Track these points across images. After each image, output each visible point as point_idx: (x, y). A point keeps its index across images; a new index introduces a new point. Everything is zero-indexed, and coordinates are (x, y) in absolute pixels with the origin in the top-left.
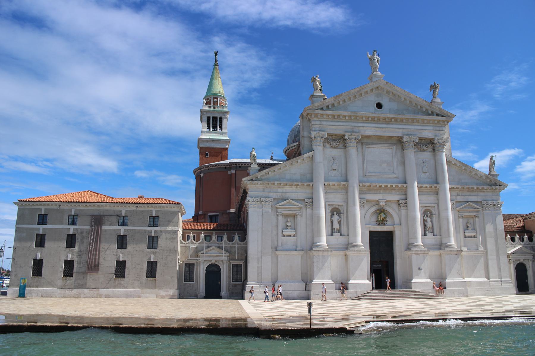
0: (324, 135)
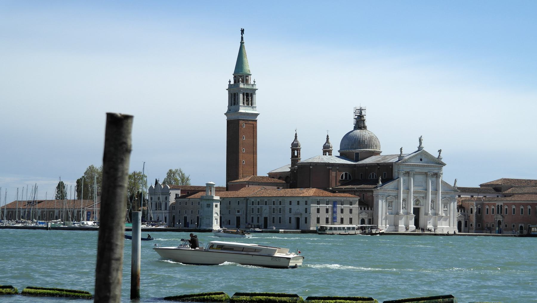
0: (404, 172)
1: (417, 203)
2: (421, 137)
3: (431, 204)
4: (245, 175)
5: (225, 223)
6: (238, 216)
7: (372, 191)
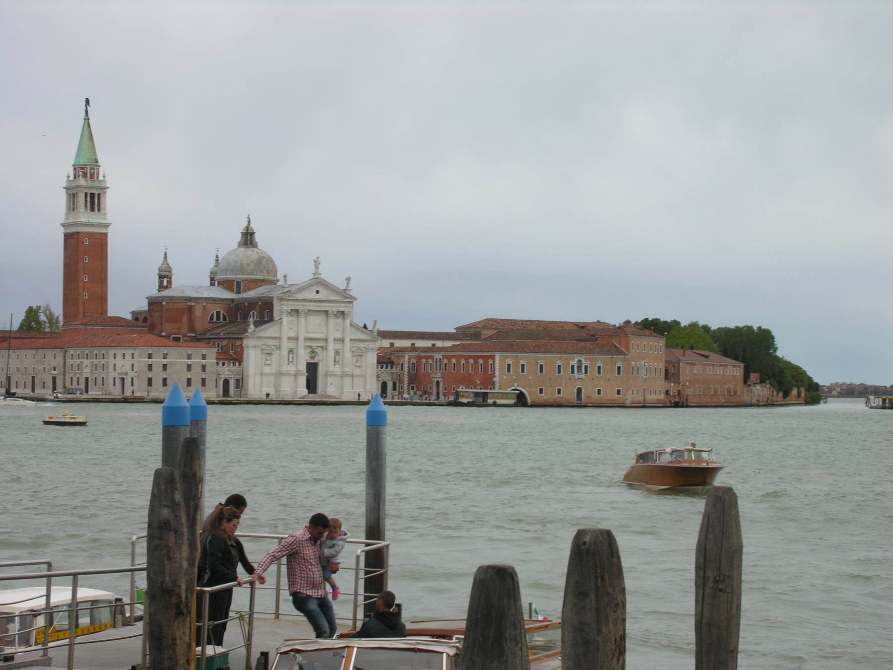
1: (312, 356)
2: (317, 259)
3: (335, 357)
4: (87, 315)
5: (39, 386)
6: (53, 376)
7: (242, 339)
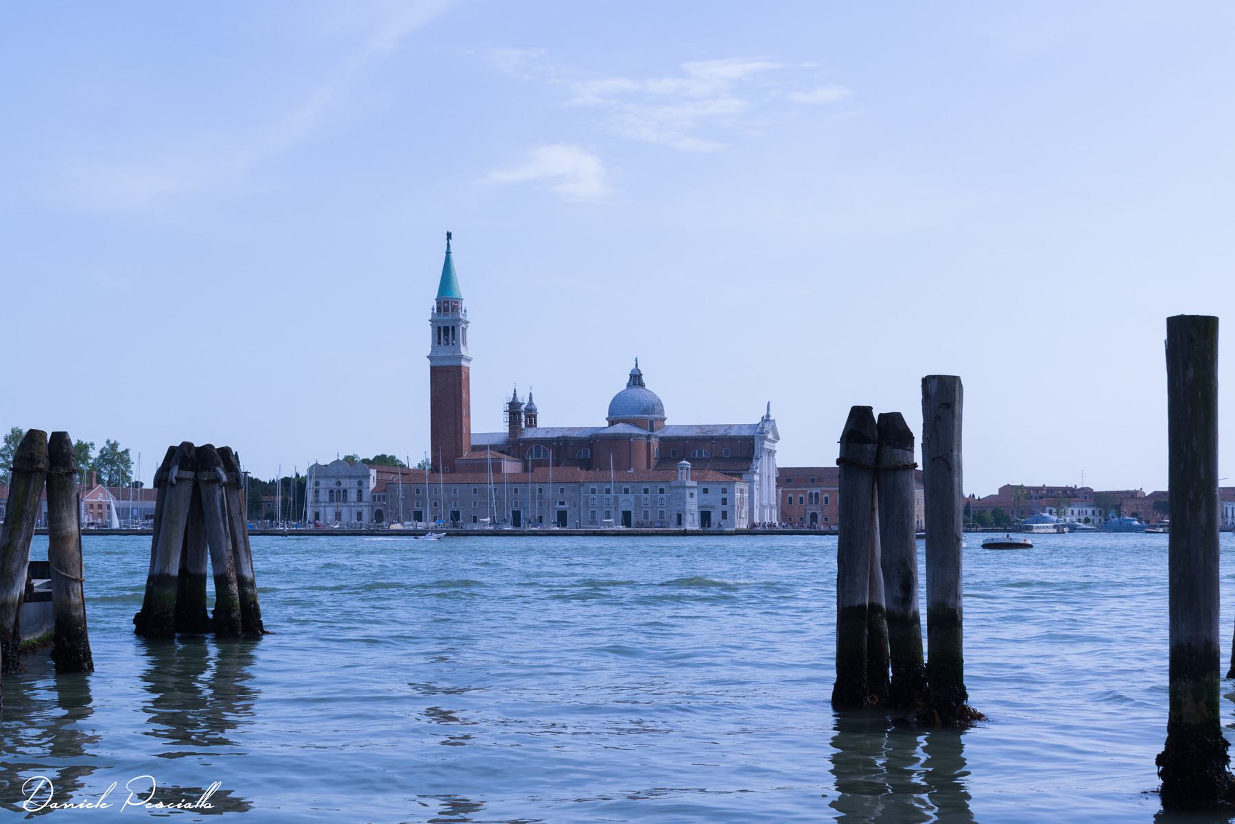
7: (741, 474)
